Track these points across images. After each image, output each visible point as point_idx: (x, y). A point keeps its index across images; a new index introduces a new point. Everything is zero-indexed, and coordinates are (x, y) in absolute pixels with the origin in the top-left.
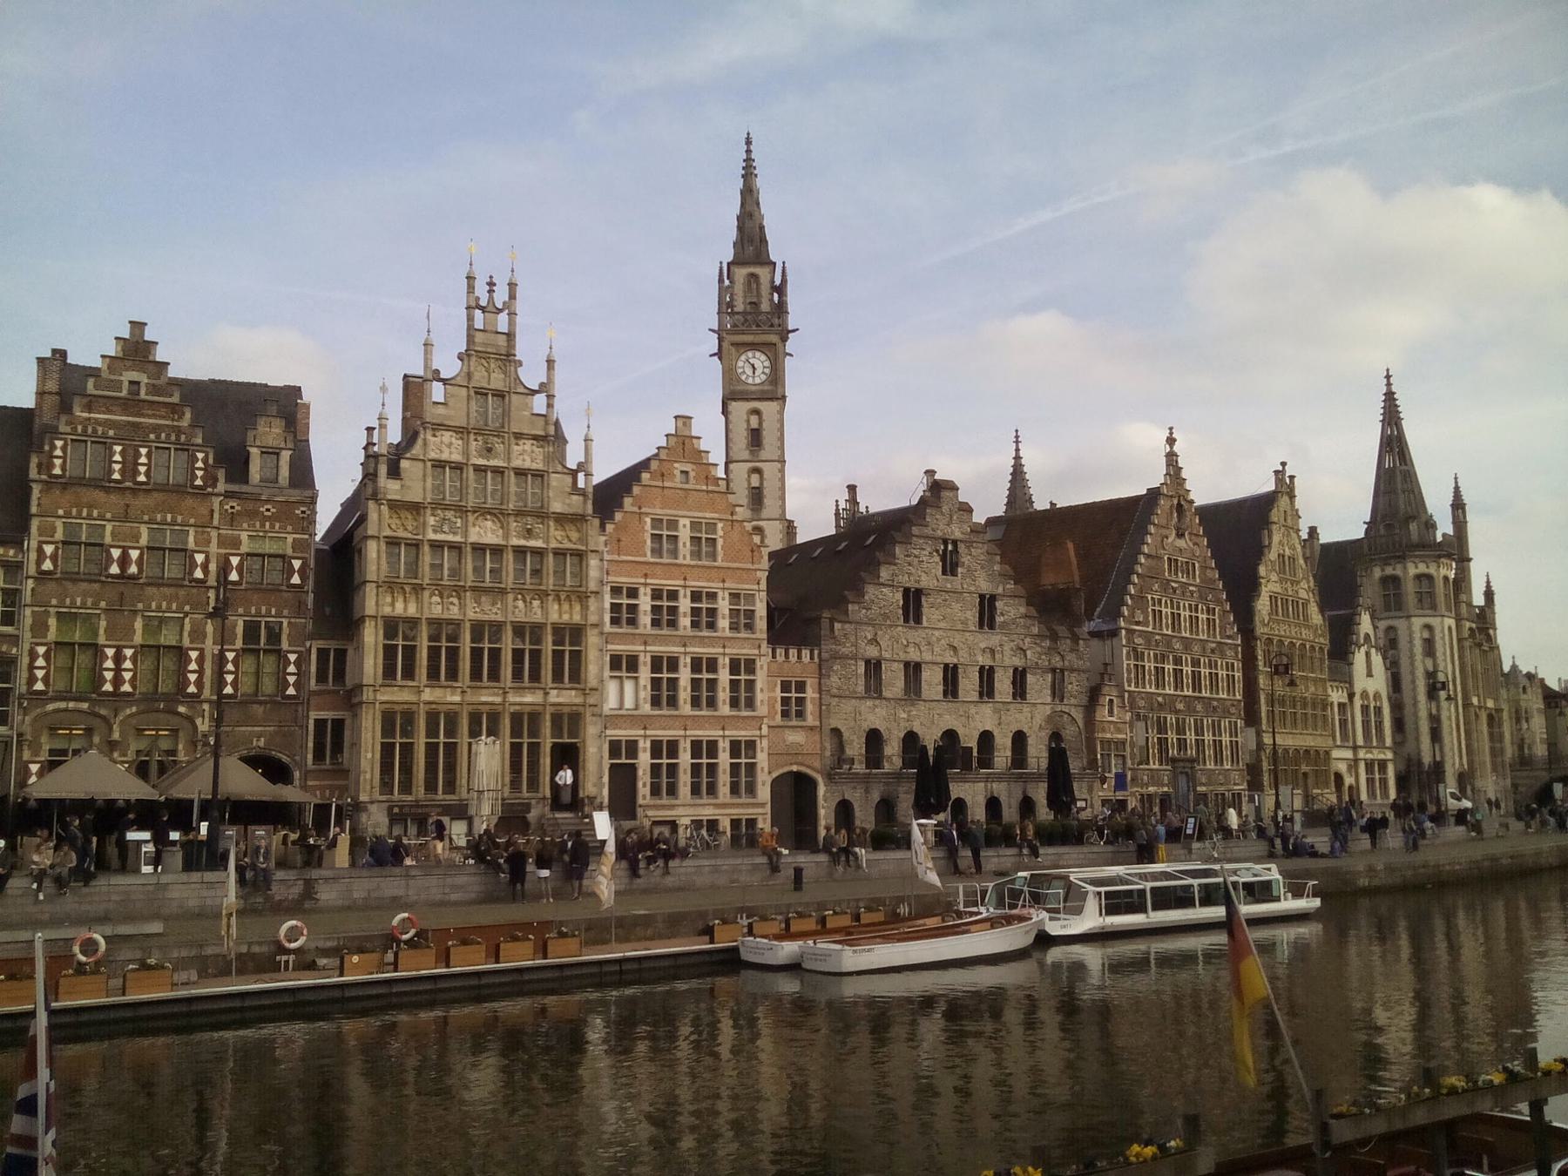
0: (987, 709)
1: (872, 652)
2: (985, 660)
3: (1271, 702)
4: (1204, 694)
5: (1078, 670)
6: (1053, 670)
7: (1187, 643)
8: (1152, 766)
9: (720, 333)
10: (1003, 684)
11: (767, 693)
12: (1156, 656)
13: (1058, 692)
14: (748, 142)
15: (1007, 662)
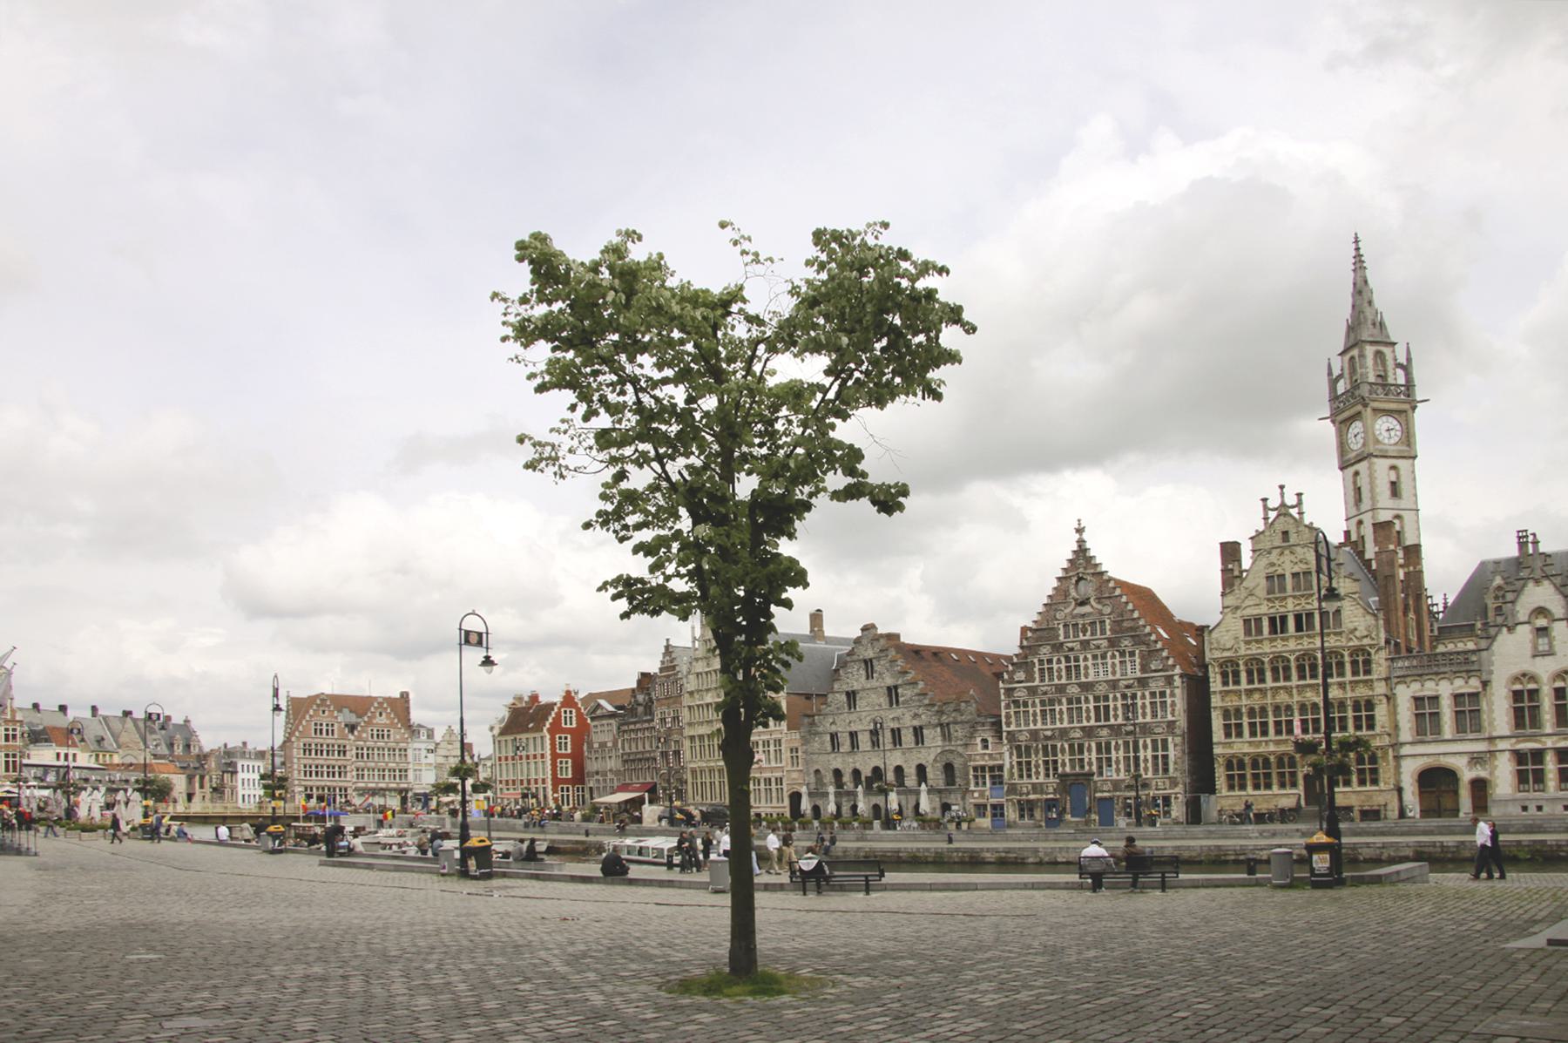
0: (898, 753)
1: (834, 729)
2: (895, 725)
3: (1226, 714)
4: (1112, 721)
5: (962, 722)
6: (941, 725)
7: (1087, 687)
8: (1034, 780)
9: (1333, 418)
10: (908, 738)
11: (786, 755)
12: (1043, 703)
13: (947, 736)
14: (1356, 242)
15: (908, 724)
